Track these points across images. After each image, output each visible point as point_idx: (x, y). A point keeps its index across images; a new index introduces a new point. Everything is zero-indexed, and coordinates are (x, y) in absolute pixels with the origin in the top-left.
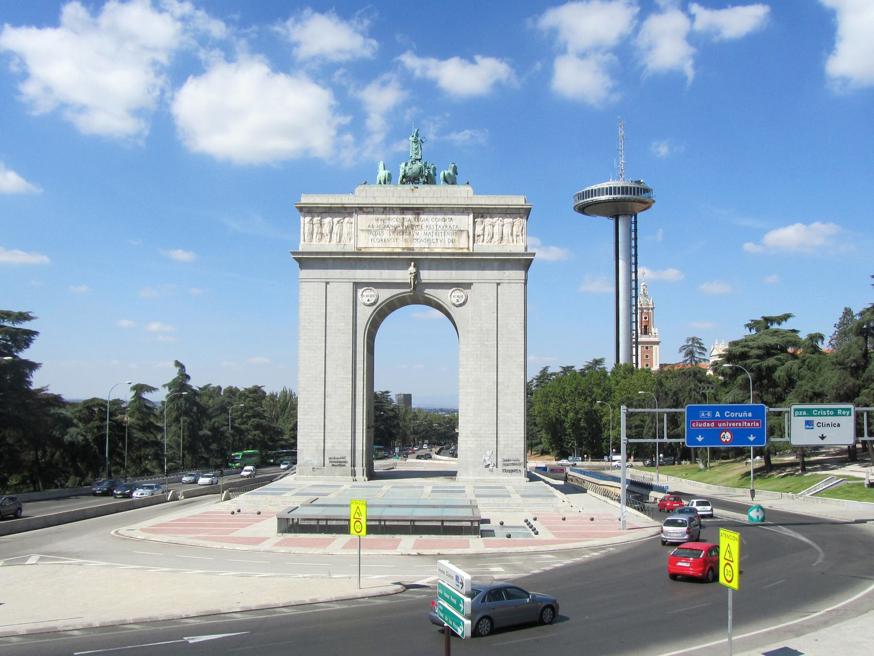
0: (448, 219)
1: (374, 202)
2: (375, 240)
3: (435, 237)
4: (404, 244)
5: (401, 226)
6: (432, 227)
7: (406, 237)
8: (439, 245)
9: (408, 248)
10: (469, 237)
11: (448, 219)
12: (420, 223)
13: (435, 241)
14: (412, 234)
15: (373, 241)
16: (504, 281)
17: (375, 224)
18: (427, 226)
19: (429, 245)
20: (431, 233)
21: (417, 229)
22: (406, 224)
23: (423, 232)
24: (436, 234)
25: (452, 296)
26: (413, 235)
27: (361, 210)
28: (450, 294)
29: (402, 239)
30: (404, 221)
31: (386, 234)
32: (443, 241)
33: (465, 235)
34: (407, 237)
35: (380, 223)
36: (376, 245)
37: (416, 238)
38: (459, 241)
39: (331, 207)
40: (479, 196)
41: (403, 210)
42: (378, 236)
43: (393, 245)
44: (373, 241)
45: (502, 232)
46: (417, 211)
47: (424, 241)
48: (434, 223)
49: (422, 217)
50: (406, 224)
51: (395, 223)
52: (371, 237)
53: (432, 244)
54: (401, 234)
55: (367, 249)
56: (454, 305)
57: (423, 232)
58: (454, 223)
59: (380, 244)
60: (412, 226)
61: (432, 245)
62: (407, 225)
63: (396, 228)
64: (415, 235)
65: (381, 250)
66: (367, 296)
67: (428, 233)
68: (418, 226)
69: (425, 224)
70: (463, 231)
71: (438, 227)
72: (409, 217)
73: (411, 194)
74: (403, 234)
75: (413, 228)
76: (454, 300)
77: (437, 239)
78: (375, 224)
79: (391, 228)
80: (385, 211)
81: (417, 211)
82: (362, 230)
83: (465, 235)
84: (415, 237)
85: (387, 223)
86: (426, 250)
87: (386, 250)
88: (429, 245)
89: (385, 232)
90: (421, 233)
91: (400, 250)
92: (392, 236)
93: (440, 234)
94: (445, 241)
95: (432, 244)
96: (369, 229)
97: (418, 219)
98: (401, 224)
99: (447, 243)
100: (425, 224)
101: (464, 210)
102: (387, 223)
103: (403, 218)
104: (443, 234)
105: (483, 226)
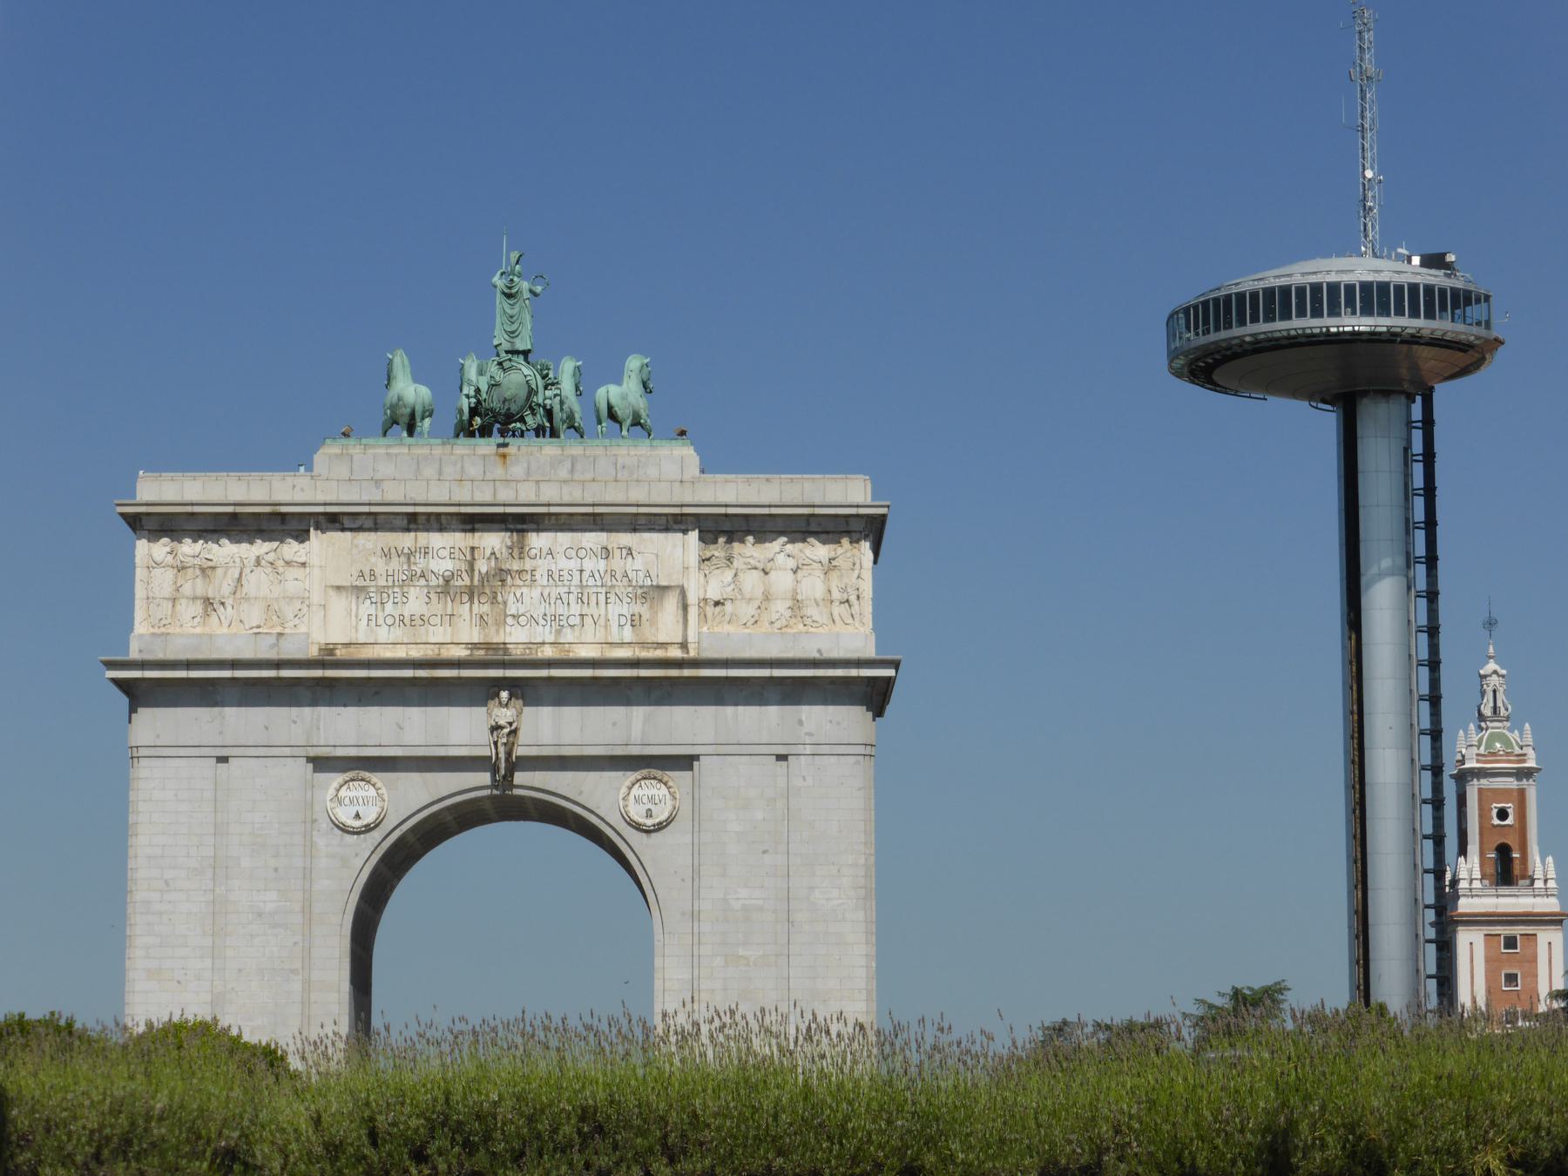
0: (617, 552)
1: (377, 498)
3: (576, 609)
6: (567, 577)
8: (589, 633)
9: (488, 646)
11: (617, 552)
12: (528, 564)
13: (575, 620)
16: (800, 749)
17: (380, 566)
19: (558, 632)
21: (519, 582)
22: (482, 566)
23: (536, 593)
26: (505, 603)
27: (333, 521)
29: (467, 617)
31: (415, 602)
32: (602, 622)
33: (671, 603)
34: (486, 608)
35: (396, 564)
36: (383, 634)
38: (653, 622)
39: (234, 515)
40: (720, 477)
41: (472, 522)
42: (389, 607)
43: (438, 634)
46: (519, 523)
48: (573, 564)
49: (538, 541)
50: (482, 566)
52: (366, 608)
53: (568, 631)
54: (466, 598)
55: (352, 650)
56: (638, 827)
57: (536, 593)
59: (398, 634)
60: (501, 574)
61: (568, 636)
63: (447, 582)
65: (400, 653)
68: (520, 572)
72: (493, 541)
73: (499, 472)
76: (637, 814)
77: (582, 615)
78: (380, 566)
79: (434, 582)
81: (519, 523)
82: (338, 588)
83: (671, 603)
84: (512, 610)
85: (420, 563)
86: (548, 653)
87: (415, 653)
88: (558, 632)
89: (413, 592)
91: (460, 653)
92: (437, 606)
93: (593, 598)
95: (568, 631)
96: (360, 583)
100: (543, 566)
101: (675, 522)
102: (420, 563)
103: (473, 549)
104: (602, 598)
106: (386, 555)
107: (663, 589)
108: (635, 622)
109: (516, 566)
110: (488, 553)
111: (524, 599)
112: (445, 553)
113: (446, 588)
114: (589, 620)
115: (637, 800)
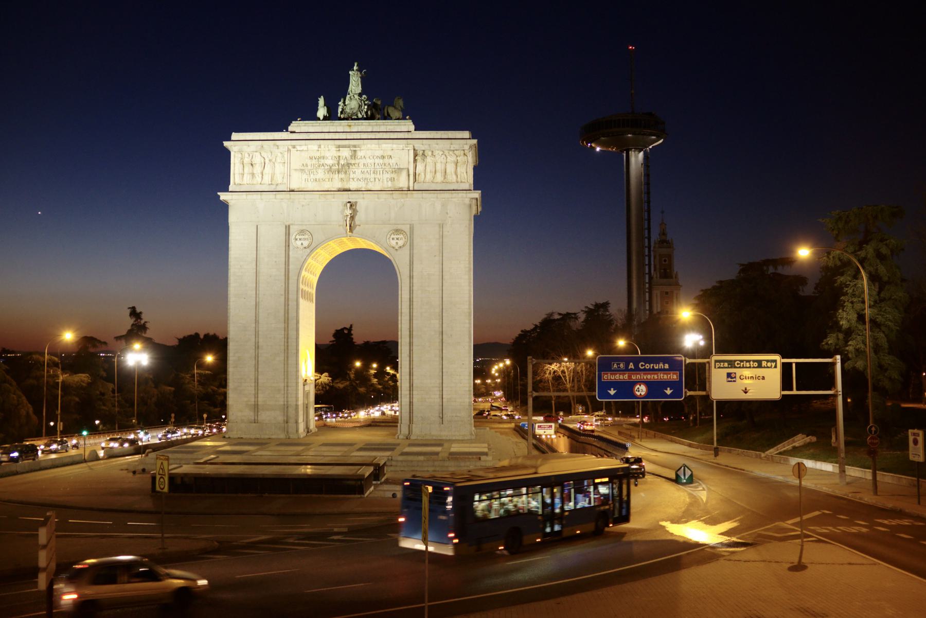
2: (309, 180)
3: (373, 176)
4: (340, 183)
5: (337, 165)
7: (342, 176)
10: (409, 175)
12: (357, 161)
13: (373, 180)
14: (348, 172)
15: (307, 181)
18: (364, 165)
19: (367, 184)
20: (369, 172)
21: (354, 167)
22: (342, 162)
23: (360, 171)
24: (374, 173)
25: (391, 238)
26: (349, 174)
28: (389, 236)
30: (339, 159)
31: (321, 174)
32: (381, 180)
33: (404, 173)
35: (314, 161)
37: (352, 177)
38: (398, 180)
42: (312, 175)
44: (307, 181)
45: (446, 170)
47: (361, 180)
48: (372, 161)
50: (342, 162)
51: (330, 162)
52: (305, 176)
54: (337, 172)
58: (392, 161)
60: (349, 165)
62: (343, 164)
63: (331, 168)
64: (351, 174)
66: (300, 239)
67: (365, 172)
68: (354, 164)
69: (362, 161)
70: (403, 169)
71: (376, 165)
74: (338, 172)
75: (349, 167)
77: (375, 179)
78: (309, 162)
79: (326, 167)
80: (319, 149)
82: (296, 170)
84: (352, 176)
88: (367, 184)
89: (320, 171)
90: (358, 171)
92: (327, 176)
93: (378, 173)
94: (383, 180)
96: (303, 168)
97: (355, 157)
98: (336, 162)
99: (385, 182)
104: (381, 172)
105: (425, 163)
106: (311, 158)
107: (400, 170)
108: (392, 180)
109: (353, 162)
110: (344, 157)
111: (356, 173)
112: (330, 158)
113: (330, 170)
114: (377, 180)
115: (393, 239)
